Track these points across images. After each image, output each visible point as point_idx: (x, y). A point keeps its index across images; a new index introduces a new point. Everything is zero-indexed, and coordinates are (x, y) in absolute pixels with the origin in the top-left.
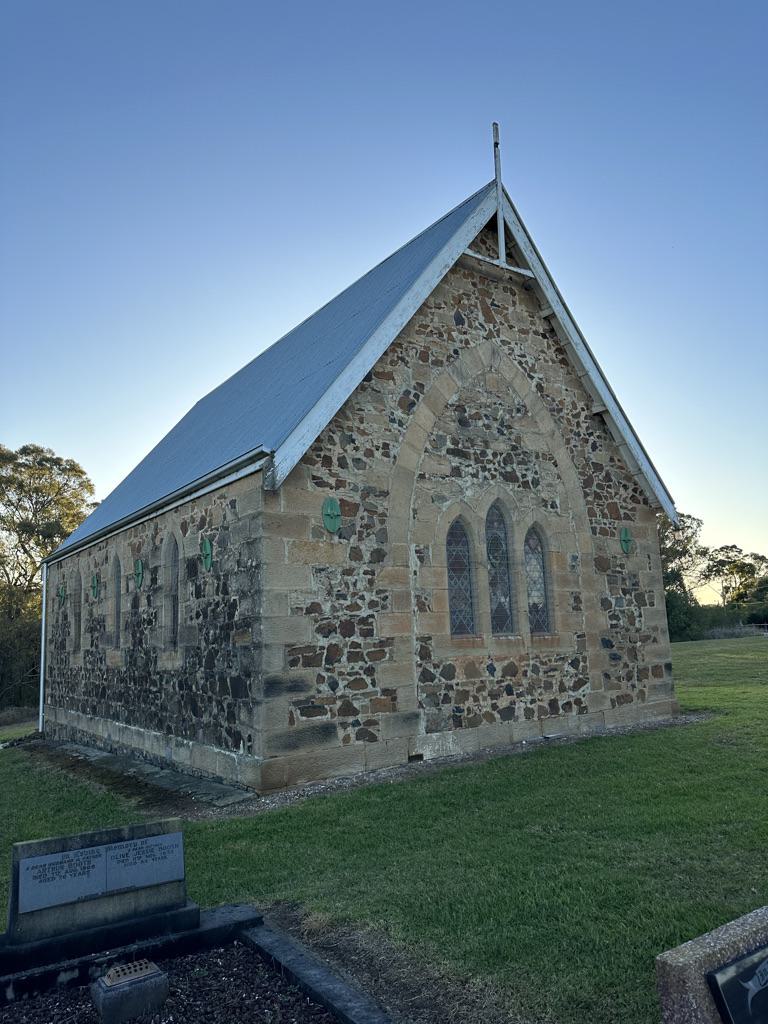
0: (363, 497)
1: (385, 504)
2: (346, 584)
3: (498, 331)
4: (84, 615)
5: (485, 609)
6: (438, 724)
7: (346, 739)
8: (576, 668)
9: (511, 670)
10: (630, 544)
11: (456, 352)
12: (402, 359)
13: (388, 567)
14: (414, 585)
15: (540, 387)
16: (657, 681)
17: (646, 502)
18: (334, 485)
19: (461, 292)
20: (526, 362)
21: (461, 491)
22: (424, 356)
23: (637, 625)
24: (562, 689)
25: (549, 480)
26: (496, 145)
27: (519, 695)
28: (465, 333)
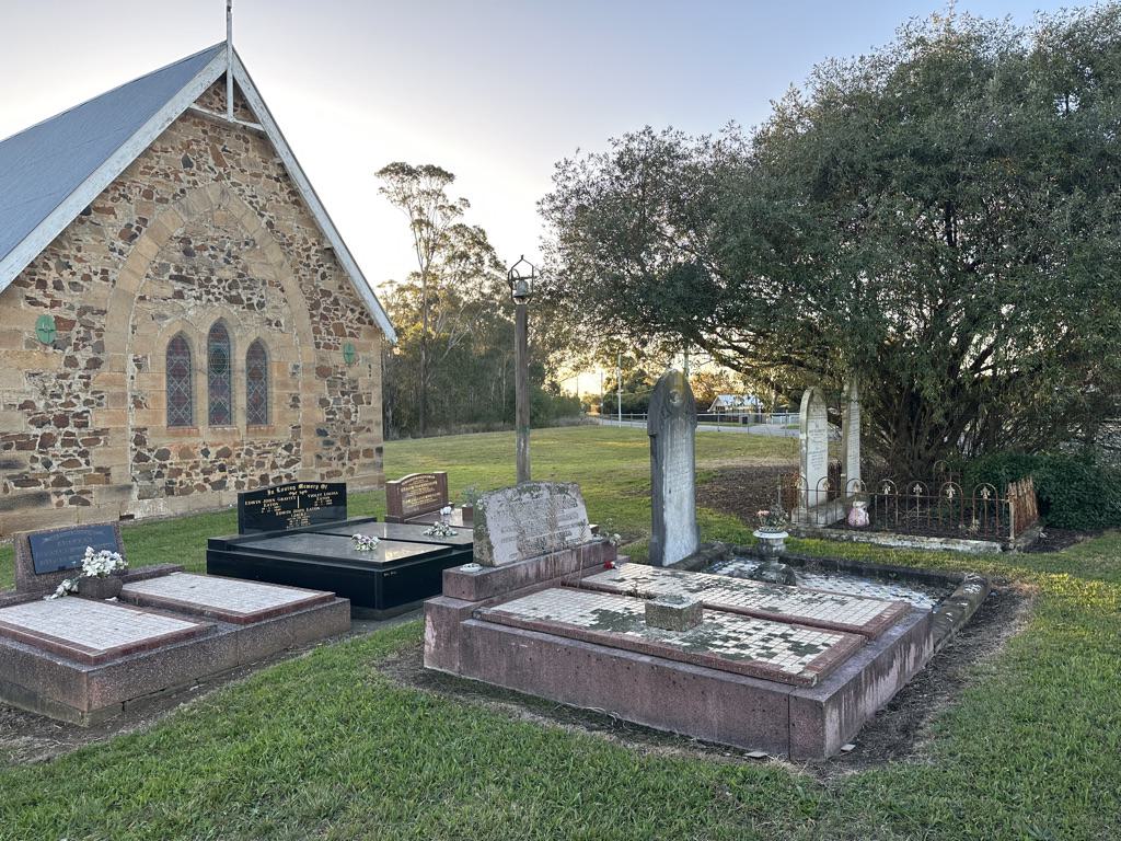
1: (103, 321)
2: (61, 386)
3: (229, 174)
5: (202, 404)
6: (150, 494)
7: (60, 504)
8: (290, 451)
9: (225, 453)
10: (352, 358)
11: (183, 191)
12: (125, 197)
13: (105, 371)
14: (130, 388)
15: (270, 224)
16: (368, 461)
17: (371, 323)
18: (49, 304)
19: (191, 138)
20: (257, 202)
21: (183, 310)
22: (148, 194)
23: (353, 419)
24: (274, 466)
25: (275, 303)
26: (229, 9)
27: (230, 472)
28: (193, 175)
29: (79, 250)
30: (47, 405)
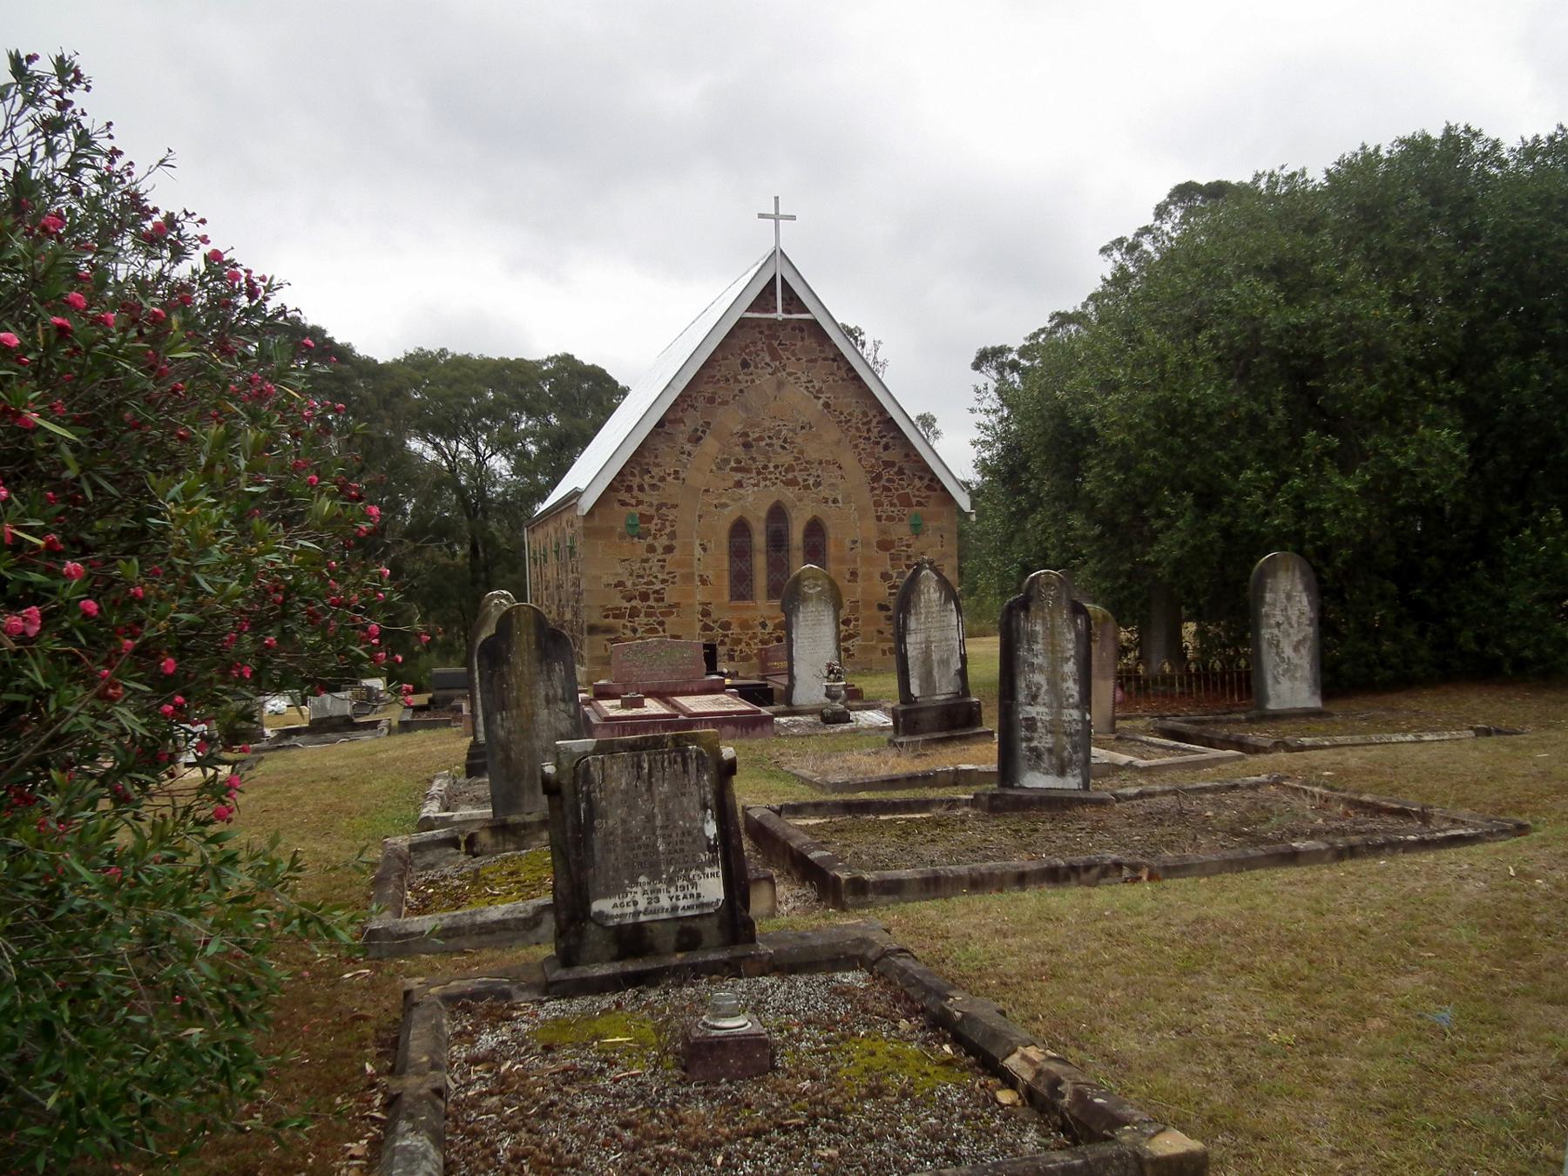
0: (657, 510)
5: (761, 580)
12: (692, 406)
13: (677, 554)
14: (698, 569)
15: (827, 405)
20: (813, 387)
29: (656, 457)
30: (634, 584)
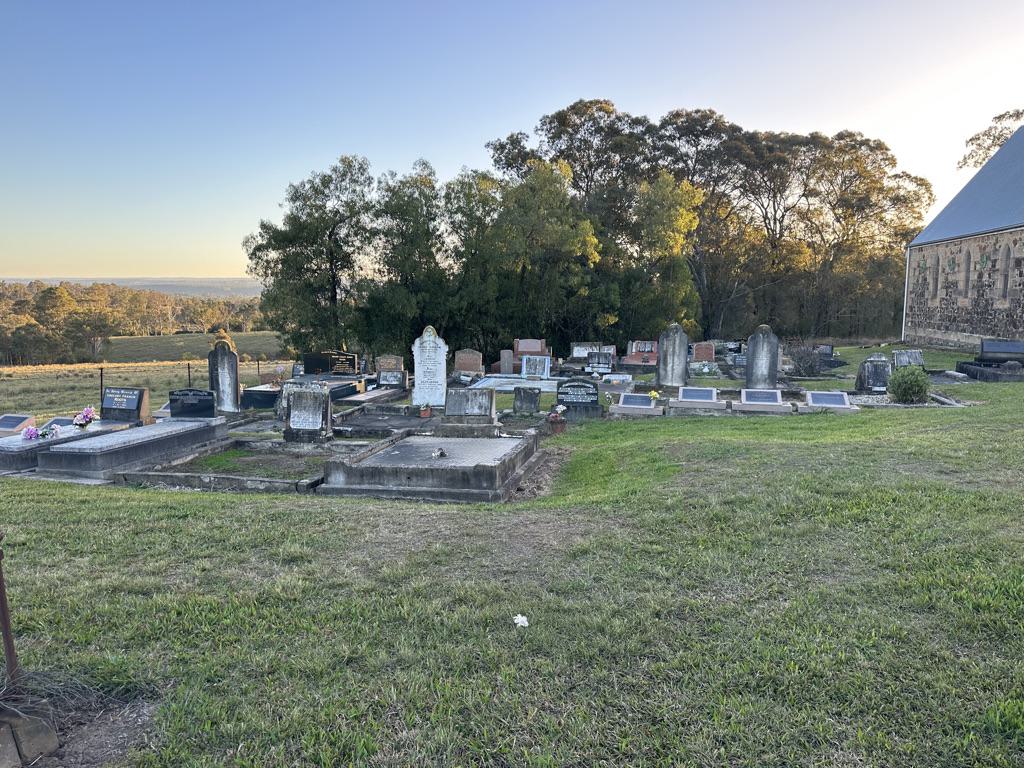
4: (941, 279)
